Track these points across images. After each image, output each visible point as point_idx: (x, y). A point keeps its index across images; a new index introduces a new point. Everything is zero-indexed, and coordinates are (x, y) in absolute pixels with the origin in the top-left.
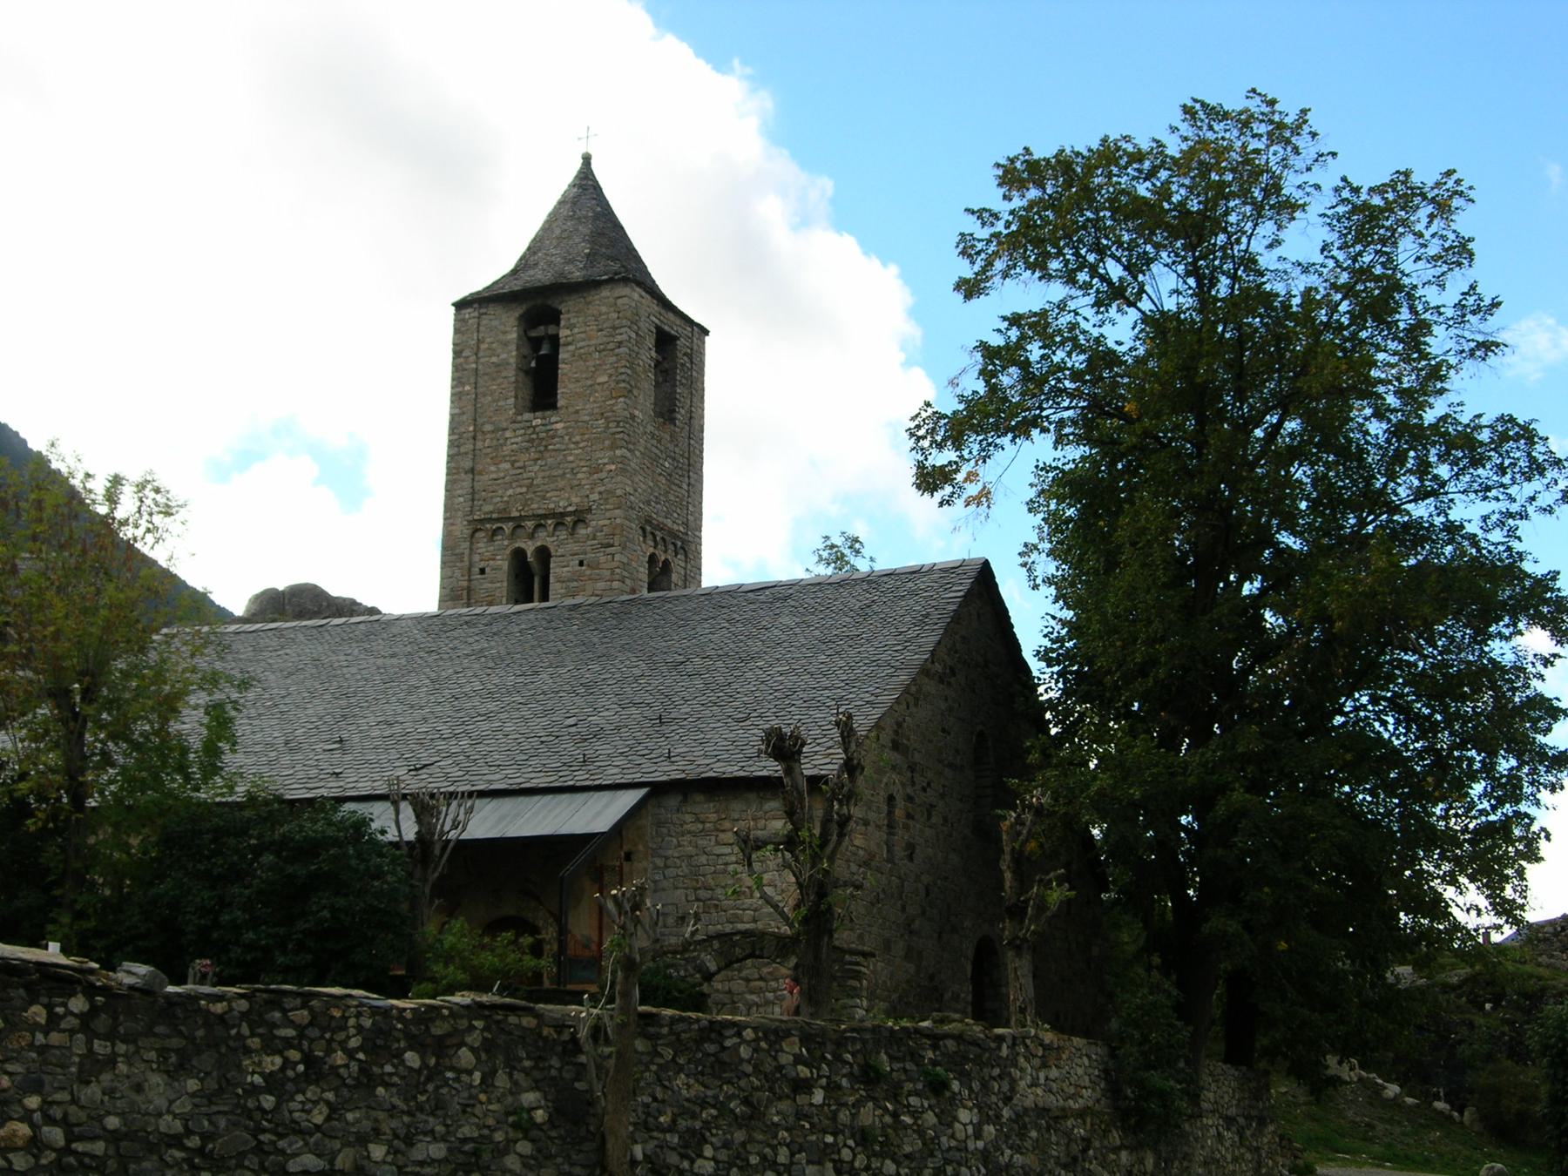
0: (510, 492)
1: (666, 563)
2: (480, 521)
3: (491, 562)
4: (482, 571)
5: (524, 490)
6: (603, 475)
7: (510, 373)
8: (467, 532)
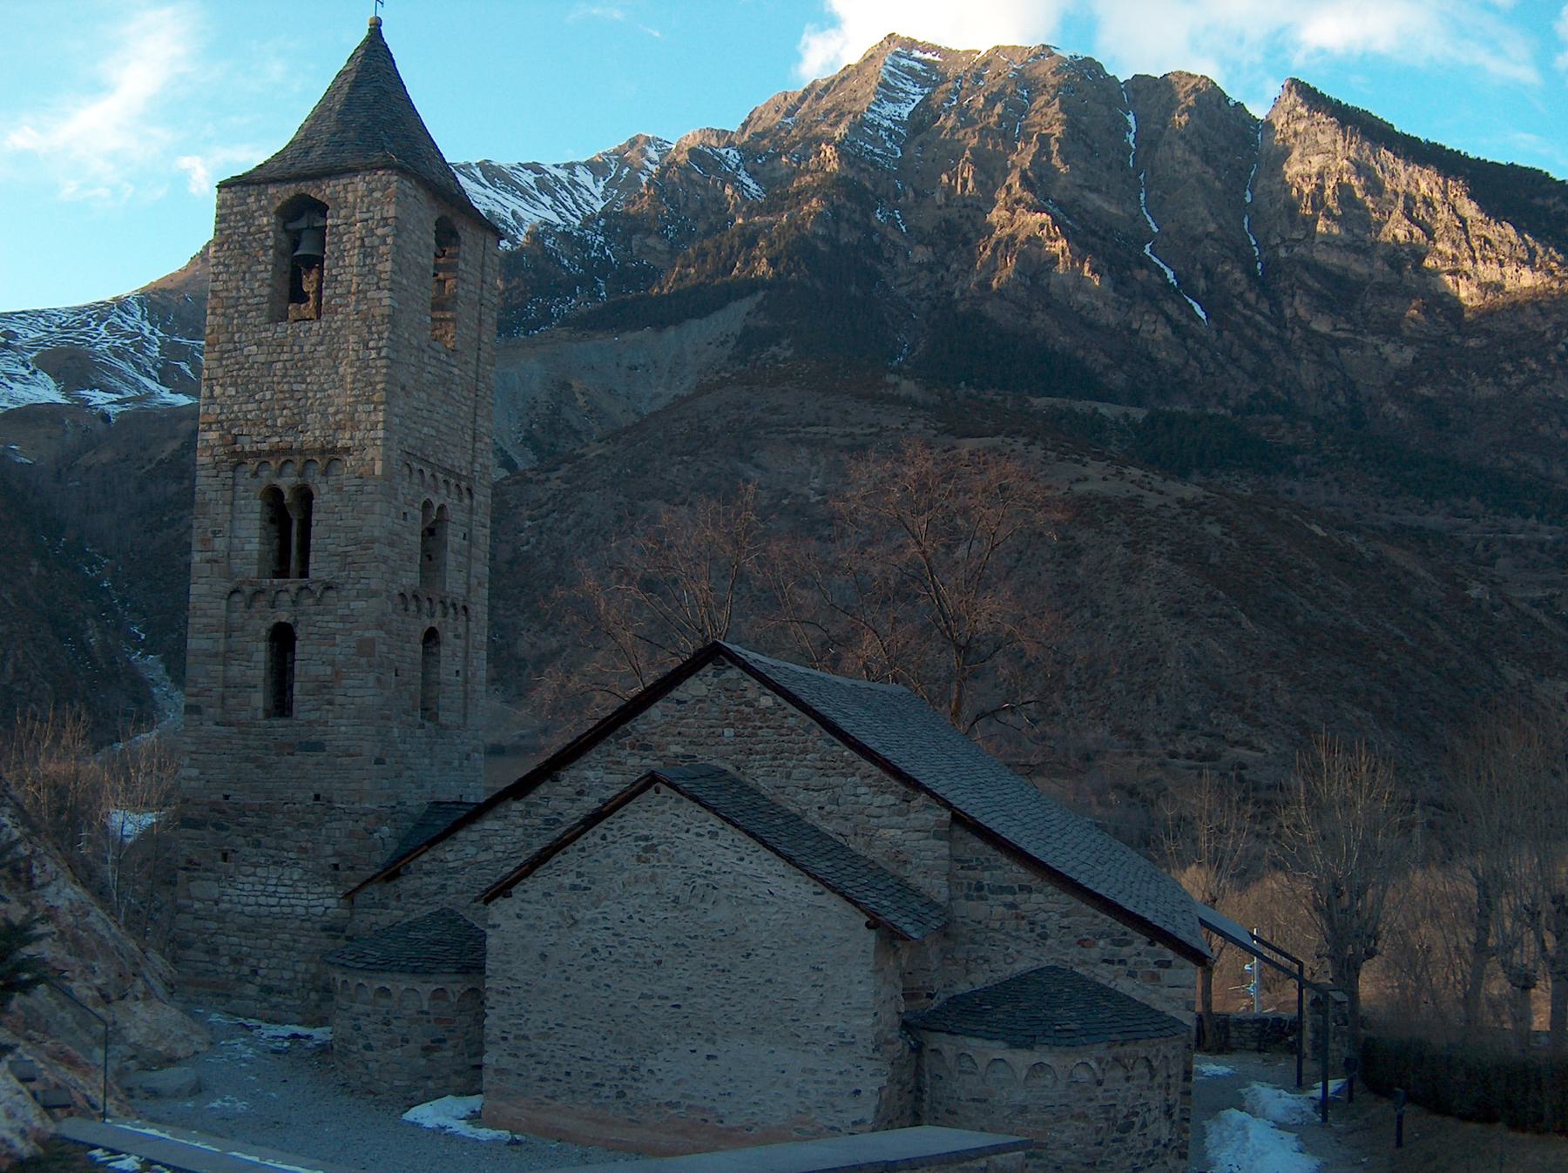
0: (425, 430)
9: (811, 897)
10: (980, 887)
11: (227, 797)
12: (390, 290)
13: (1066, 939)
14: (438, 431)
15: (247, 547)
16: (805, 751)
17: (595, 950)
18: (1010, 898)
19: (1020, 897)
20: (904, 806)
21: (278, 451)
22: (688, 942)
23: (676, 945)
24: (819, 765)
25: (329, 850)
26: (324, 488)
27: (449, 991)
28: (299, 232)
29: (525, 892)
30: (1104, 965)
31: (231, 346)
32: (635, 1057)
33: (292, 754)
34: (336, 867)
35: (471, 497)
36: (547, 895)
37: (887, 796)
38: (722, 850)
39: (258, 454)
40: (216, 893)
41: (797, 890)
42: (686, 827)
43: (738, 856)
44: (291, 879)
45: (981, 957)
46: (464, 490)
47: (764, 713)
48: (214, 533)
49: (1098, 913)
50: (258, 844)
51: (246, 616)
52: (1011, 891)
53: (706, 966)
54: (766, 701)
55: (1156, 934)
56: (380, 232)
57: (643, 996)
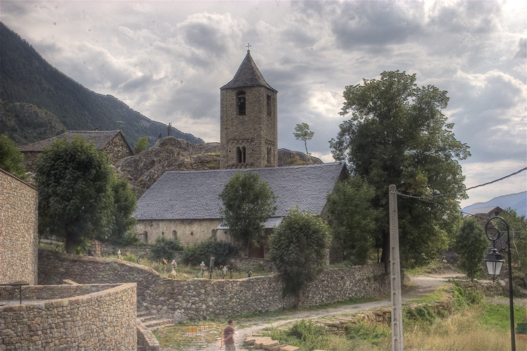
1: (270, 148)
2: (229, 140)
4: (230, 151)
7: (235, 106)
8: (226, 142)
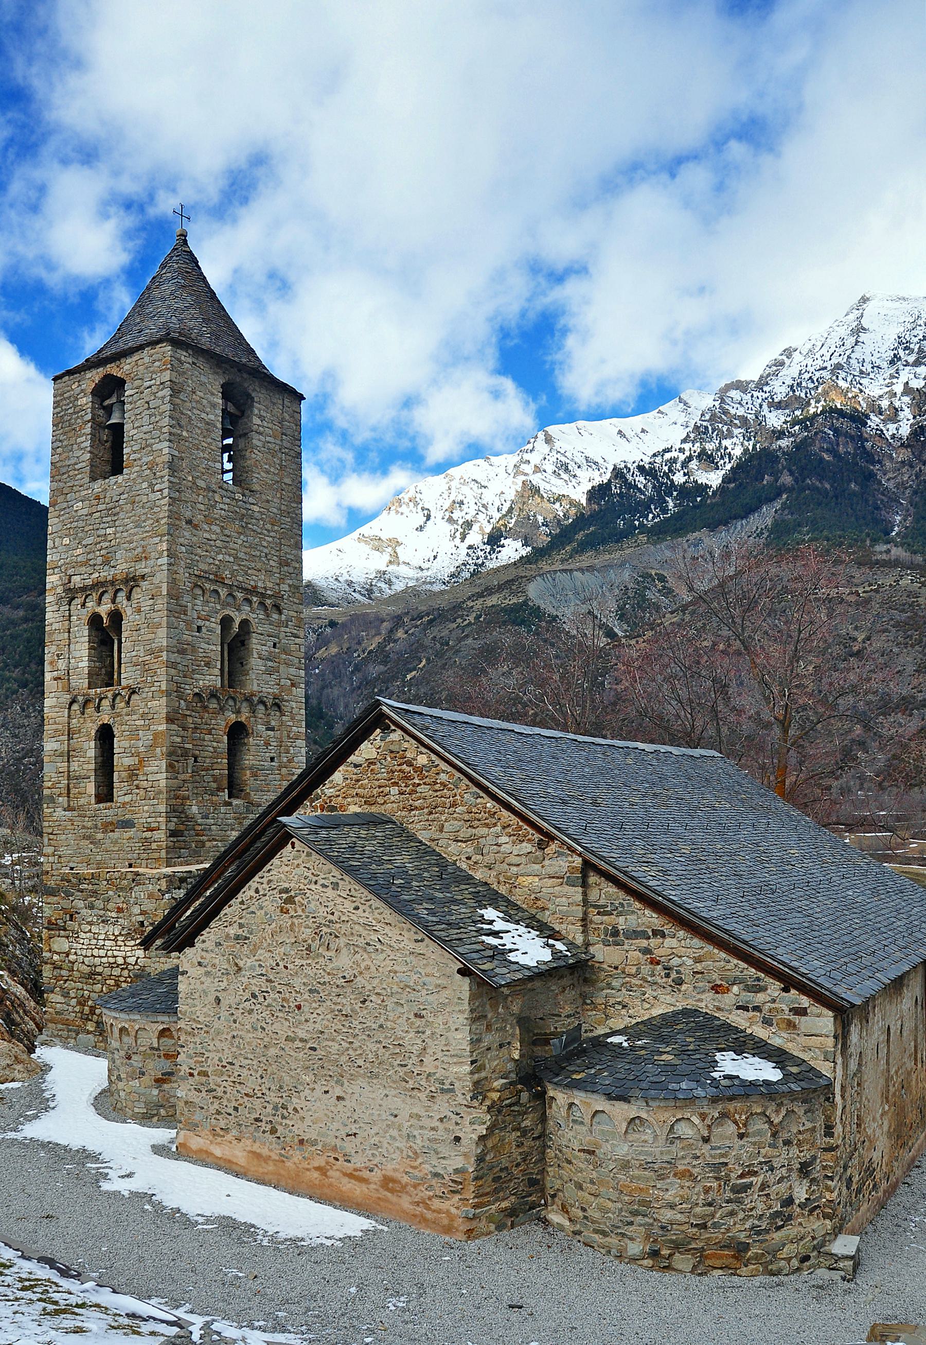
0: (220, 557)
3: (207, 623)
4: (199, 629)
5: (232, 559)
6: (291, 570)
9: (412, 945)
10: (615, 933)
11: (72, 869)
12: (170, 441)
13: (701, 984)
14: (236, 558)
15: (80, 665)
16: (454, 805)
17: (254, 996)
18: (644, 943)
19: (654, 942)
20: (539, 853)
21: (97, 584)
22: (320, 988)
23: (310, 991)
24: (467, 817)
25: (136, 910)
26: (129, 611)
27: (172, 1029)
28: (112, 404)
29: (204, 941)
30: (739, 1012)
31: (65, 505)
32: (284, 1095)
33: (113, 831)
34: (142, 924)
35: (280, 613)
36: (218, 944)
37: (524, 844)
38: (341, 899)
39: (84, 589)
40: (66, 947)
41: (400, 938)
42: (314, 879)
43: (354, 905)
44: (113, 934)
45: (619, 1003)
46: (270, 607)
47: (419, 770)
48: (58, 655)
49: (728, 958)
50: (92, 907)
51: (82, 720)
52: (644, 935)
53: (333, 1011)
54: (422, 760)
55: (789, 982)
56: (160, 394)
57: (288, 1039)
